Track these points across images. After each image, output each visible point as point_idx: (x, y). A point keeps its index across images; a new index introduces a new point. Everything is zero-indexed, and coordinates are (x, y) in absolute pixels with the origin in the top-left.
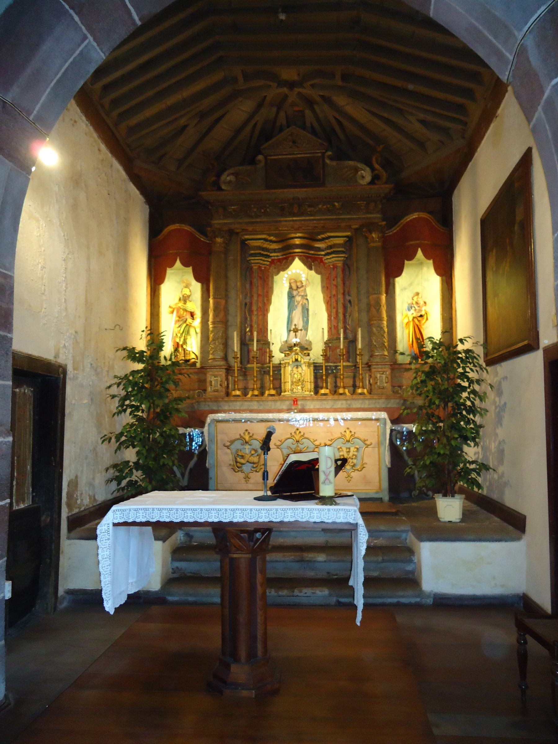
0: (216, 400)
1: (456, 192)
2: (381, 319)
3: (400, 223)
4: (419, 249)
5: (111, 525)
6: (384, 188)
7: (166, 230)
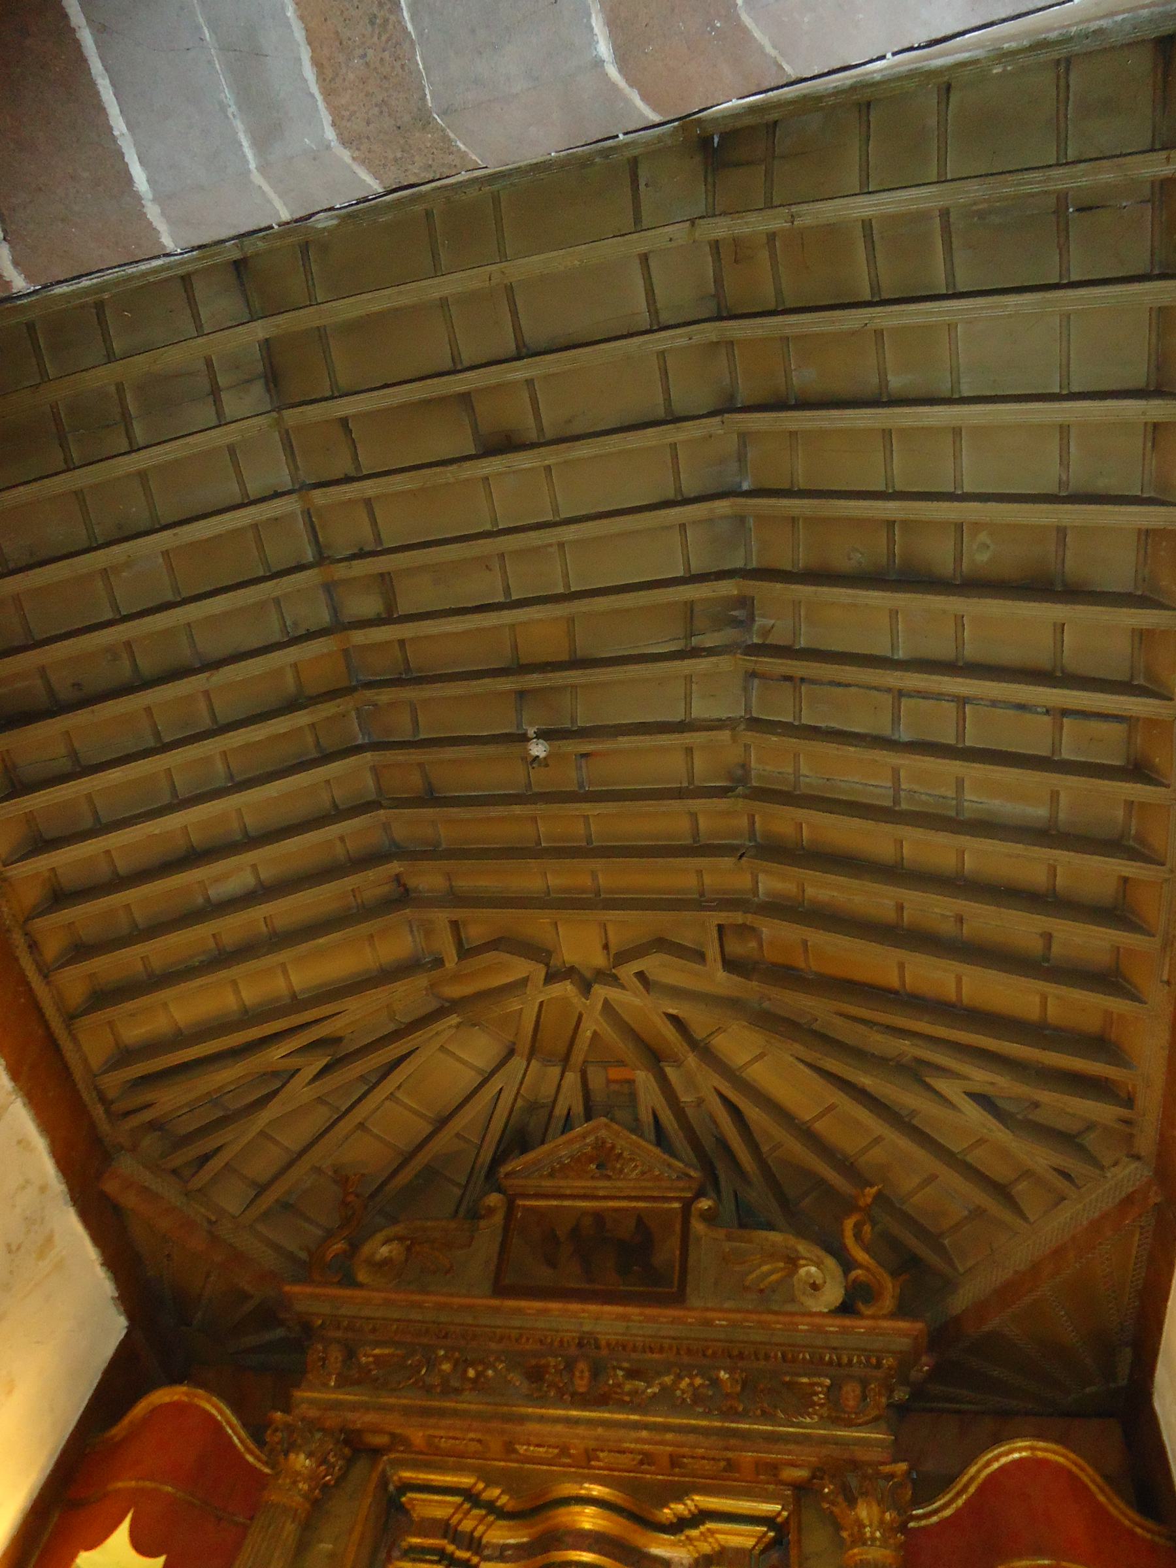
6: (889, 1331)
7: (141, 1408)
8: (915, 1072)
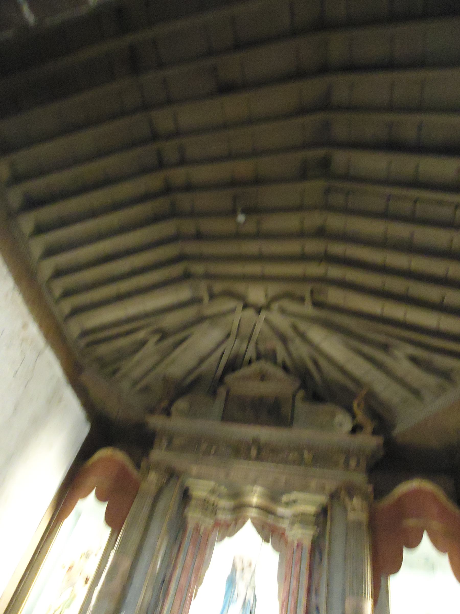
6: (369, 441)
8: (385, 347)
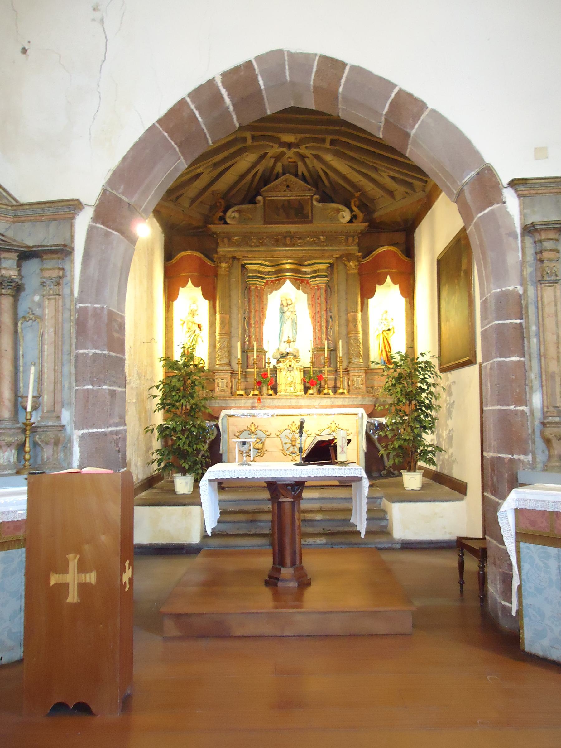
0: (224, 398)
1: (417, 230)
2: (357, 333)
3: (372, 254)
4: (388, 276)
5: (207, 481)
6: (360, 226)
7: (179, 256)
